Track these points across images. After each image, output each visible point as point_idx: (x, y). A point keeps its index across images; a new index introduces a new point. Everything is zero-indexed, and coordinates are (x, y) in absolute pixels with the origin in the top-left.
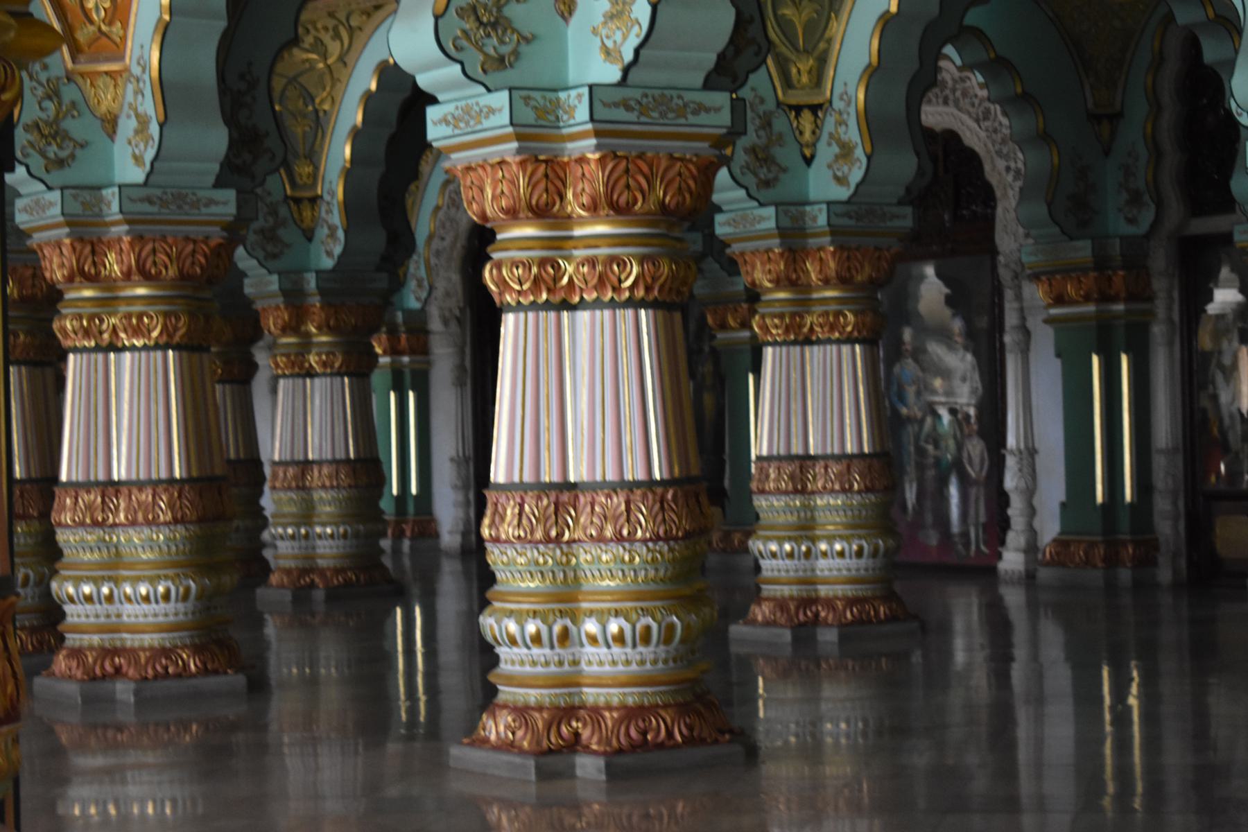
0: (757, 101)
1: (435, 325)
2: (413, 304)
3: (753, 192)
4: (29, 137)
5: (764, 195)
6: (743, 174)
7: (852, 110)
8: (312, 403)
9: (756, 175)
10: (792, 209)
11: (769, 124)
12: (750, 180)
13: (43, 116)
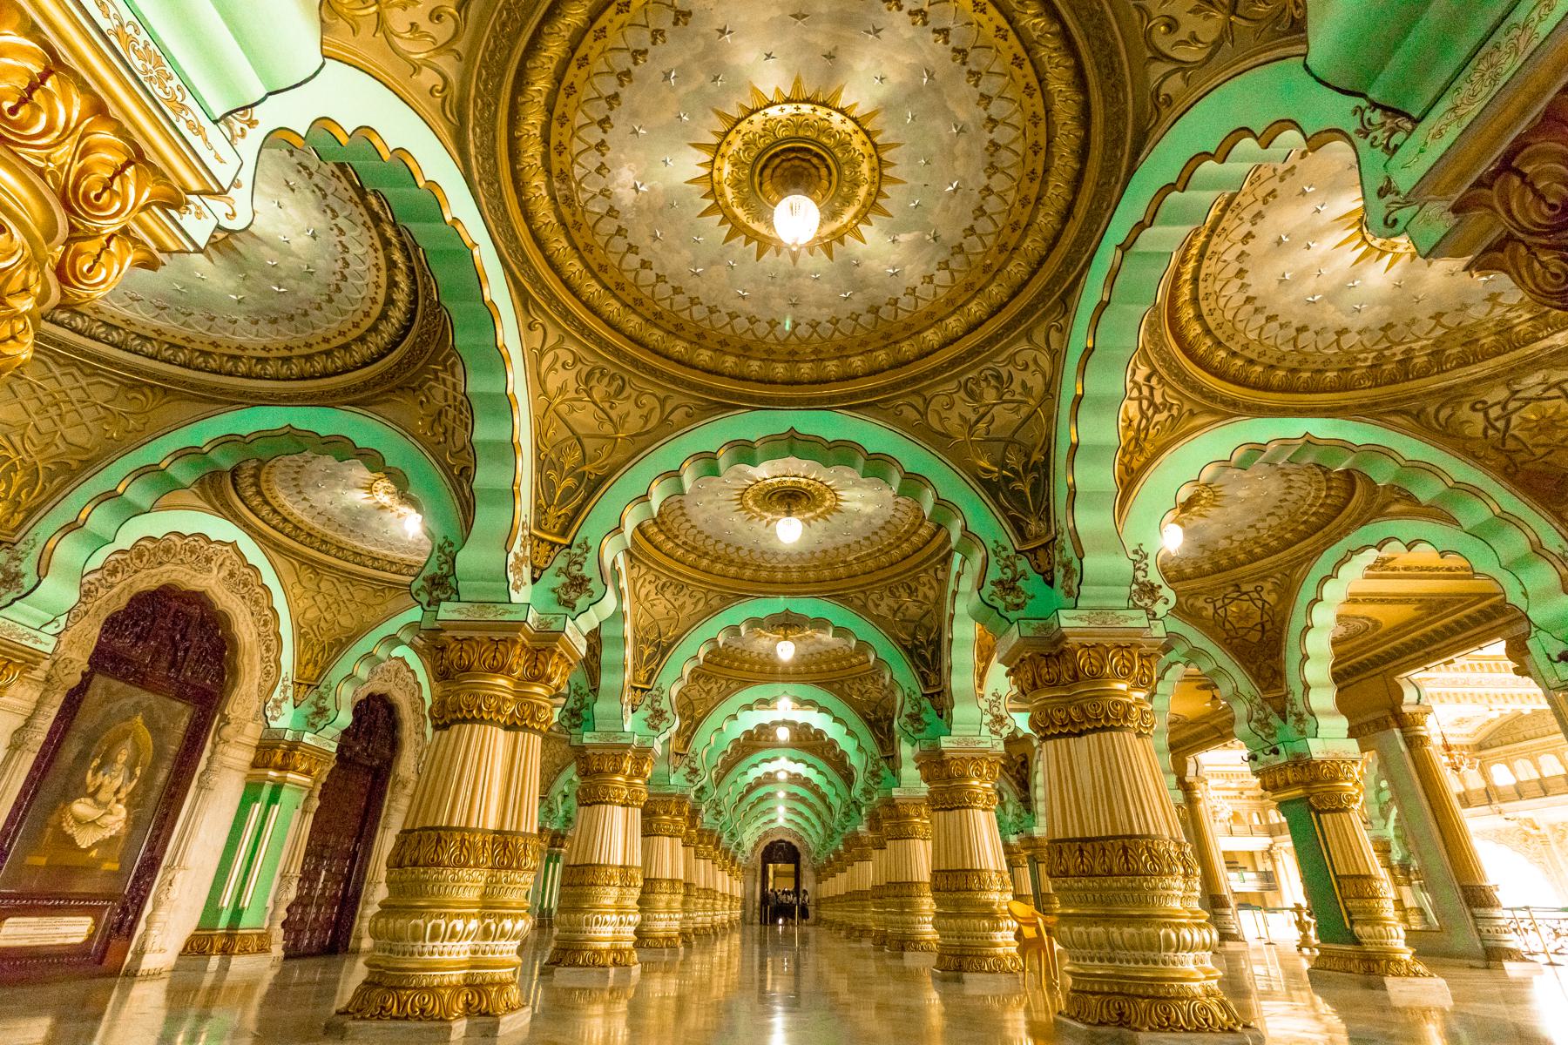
3: (1002, 611)
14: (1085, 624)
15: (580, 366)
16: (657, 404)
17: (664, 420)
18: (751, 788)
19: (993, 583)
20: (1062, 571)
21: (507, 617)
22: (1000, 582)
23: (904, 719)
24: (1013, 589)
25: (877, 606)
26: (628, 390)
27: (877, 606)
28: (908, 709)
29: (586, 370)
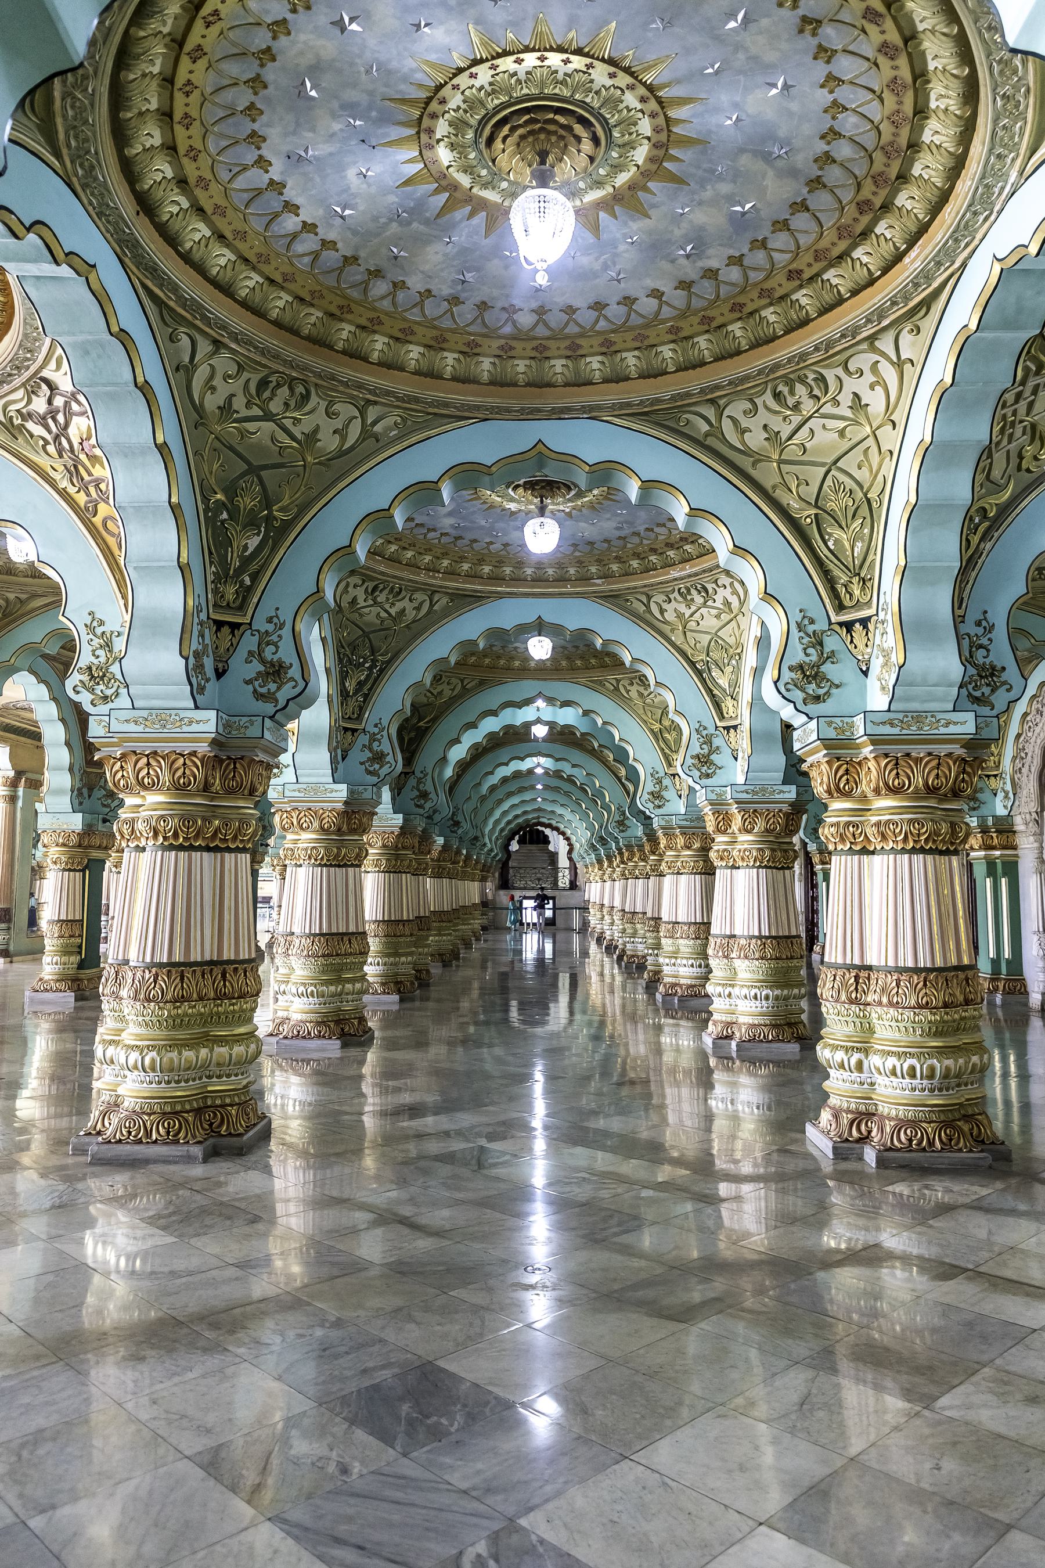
0: (806, 622)
1: (1019, 827)
2: (1001, 811)
4: (82, 677)
5: (812, 708)
6: (788, 690)
7: (889, 617)
8: (871, 876)
9: (803, 690)
10: (838, 720)
11: (821, 644)
12: (798, 695)
13: (96, 661)
14: (896, 731)
15: (246, 375)
16: (357, 414)
17: (367, 433)
18: (493, 789)
19: (791, 669)
20: (881, 660)
21: (195, 727)
22: (801, 667)
23: (689, 761)
24: (815, 677)
25: (662, 611)
26: (314, 400)
27: (662, 611)
28: (696, 749)
29: (255, 378)
